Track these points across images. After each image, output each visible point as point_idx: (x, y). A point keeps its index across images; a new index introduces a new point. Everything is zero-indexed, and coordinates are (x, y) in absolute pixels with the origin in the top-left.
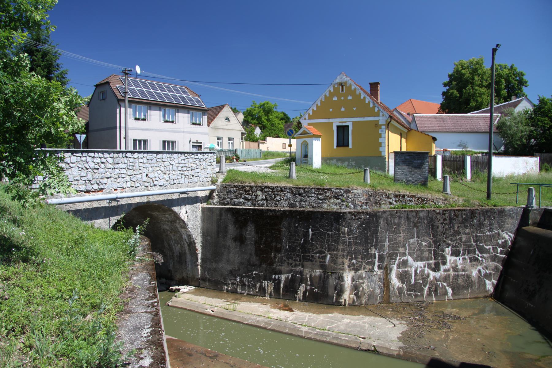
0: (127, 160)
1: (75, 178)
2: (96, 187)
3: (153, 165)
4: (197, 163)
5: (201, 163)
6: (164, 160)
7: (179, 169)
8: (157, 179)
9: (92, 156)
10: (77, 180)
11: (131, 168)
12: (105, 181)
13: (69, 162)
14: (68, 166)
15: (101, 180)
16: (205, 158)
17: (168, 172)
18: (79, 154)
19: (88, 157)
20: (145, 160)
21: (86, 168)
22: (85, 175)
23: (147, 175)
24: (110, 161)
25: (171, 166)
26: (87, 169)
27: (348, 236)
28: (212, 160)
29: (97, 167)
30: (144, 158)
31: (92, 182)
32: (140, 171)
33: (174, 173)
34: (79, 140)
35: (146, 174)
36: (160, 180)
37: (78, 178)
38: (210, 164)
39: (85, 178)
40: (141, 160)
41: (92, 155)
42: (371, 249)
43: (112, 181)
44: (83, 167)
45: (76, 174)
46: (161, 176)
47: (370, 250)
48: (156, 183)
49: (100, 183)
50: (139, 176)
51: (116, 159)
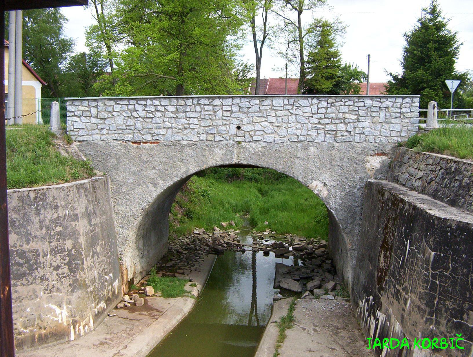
0: (202, 108)
1: (118, 127)
2: (149, 138)
3: (250, 114)
4: (361, 113)
5: (373, 114)
6: (275, 108)
7: (311, 122)
8: (262, 133)
9: (144, 104)
10: (122, 130)
11: (206, 117)
12: (162, 132)
13: (111, 110)
14: (110, 115)
15: (156, 131)
16: (384, 105)
17: (284, 125)
18: (126, 102)
19: (136, 105)
20: (235, 108)
21: (133, 116)
22: (131, 124)
23: (239, 128)
24: (172, 109)
25: (294, 117)
26: (137, 118)
27: (433, 269)
28: (404, 110)
29: (151, 116)
30: (233, 106)
31: (142, 133)
32: (225, 122)
33: (299, 126)
34: (450, 90)
35: (236, 126)
36: (266, 136)
37: (124, 127)
38: (399, 115)
39: (133, 128)
40: (229, 108)
41: (143, 102)
42: (468, 315)
43: (174, 132)
44: (130, 115)
45: (119, 122)
46: (269, 128)
47: (465, 316)
48: (255, 138)
49: (155, 133)
50: (223, 128)
51: (181, 107)
